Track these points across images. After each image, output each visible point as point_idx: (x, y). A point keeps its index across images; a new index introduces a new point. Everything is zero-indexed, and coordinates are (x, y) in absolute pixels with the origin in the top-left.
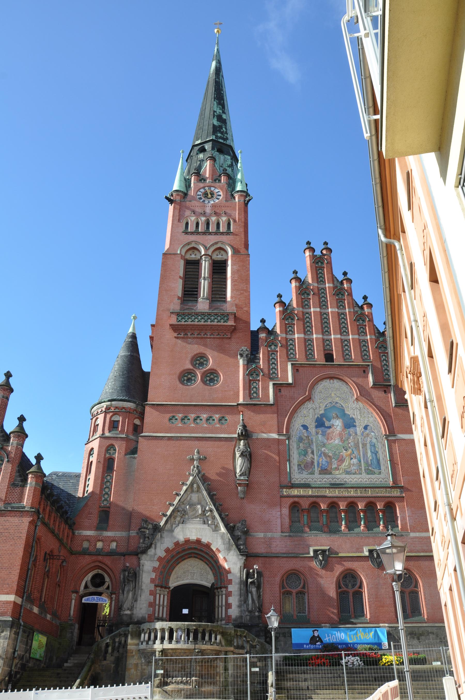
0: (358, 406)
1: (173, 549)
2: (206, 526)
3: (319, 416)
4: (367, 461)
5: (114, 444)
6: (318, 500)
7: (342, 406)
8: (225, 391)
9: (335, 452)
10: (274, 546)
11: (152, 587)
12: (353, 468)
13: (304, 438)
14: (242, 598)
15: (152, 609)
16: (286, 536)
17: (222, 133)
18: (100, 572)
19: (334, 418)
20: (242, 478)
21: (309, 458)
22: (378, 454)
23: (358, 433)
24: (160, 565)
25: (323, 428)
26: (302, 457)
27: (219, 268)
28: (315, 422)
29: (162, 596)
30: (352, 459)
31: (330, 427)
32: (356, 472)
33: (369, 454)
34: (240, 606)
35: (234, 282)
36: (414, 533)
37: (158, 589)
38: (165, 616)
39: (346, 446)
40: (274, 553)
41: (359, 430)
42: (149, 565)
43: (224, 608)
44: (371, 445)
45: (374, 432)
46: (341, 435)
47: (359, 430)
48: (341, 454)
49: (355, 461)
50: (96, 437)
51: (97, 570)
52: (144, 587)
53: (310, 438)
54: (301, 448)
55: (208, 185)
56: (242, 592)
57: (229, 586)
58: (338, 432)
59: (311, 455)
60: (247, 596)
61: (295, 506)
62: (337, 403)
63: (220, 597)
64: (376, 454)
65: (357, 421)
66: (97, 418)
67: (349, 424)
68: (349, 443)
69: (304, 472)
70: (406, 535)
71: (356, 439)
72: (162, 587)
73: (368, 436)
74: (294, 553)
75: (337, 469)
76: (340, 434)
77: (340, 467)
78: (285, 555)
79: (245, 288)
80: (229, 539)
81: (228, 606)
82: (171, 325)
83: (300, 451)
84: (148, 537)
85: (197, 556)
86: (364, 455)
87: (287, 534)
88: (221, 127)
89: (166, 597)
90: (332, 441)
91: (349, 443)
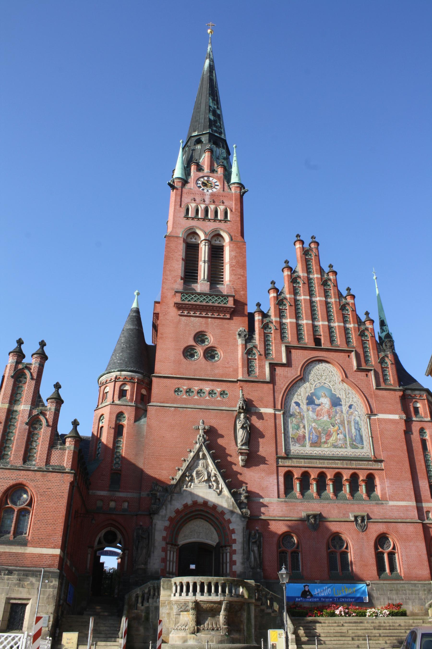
0: (343, 387)
1: (183, 511)
2: (211, 491)
3: (310, 395)
4: (352, 437)
5: (124, 411)
7: (330, 387)
8: (225, 367)
9: (324, 427)
10: (272, 510)
11: (163, 544)
12: (340, 443)
13: (297, 414)
14: (245, 556)
15: (164, 564)
16: (282, 501)
17: (216, 127)
18: (113, 529)
19: (322, 397)
20: (244, 447)
21: (301, 432)
22: (361, 431)
23: (344, 411)
24: (170, 525)
25: (313, 405)
26: (295, 431)
27: (216, 253)
28: (306, 400)
29: (172, 553)
30: (338, 434)
31: (319, 405)
32: (342, 446)
33: (353, 430)
34: (243, 563)
35: (232, 267)
36: (392, 502)
37: (169, 546)
38: (174, 571)
39: (334, 422)
40: (271, 516)
41: (345, 408)
42: (160, 525)
43: (228, 565)
44: (355, 423)
45: (357, 411)
46: (329, 413)
47: (345, 408)
48: (329, 429)
50: (106, 404)
51: (109, 528)
52: (157, 544)
53: (302, 414)
54: (294, 422)
55: (207, 175)
56: (245, 550)
57: (234, 545)
58: (326, 409)
59: (303, 430)
60: (249, 554)
62: (325, 383)
63: (225, 555)
64: (359, 431)
65: (342, 401)
66: (106, 386)
67: (336, 402)
68: (336, 420)
69: (297, 444)
70: (386, 503)
71: (342, 417)
72: (172, 545)
73: (352, 415)
74: (290, 517)
75: (326, 443)
76: (328, 412)
77: (328, 441)
78: (282, 519)
79: (242, 274)
80: (233, 503)
81: (233, 563)
82: (175, 303)
83: (293, 425)
84: (159, 499)
85: (203, 517)
86: (349, 431)
87: (283, 500)
88: (215, 121)
89: (175, 553)
90: (321, 417)
91: (336, 420)
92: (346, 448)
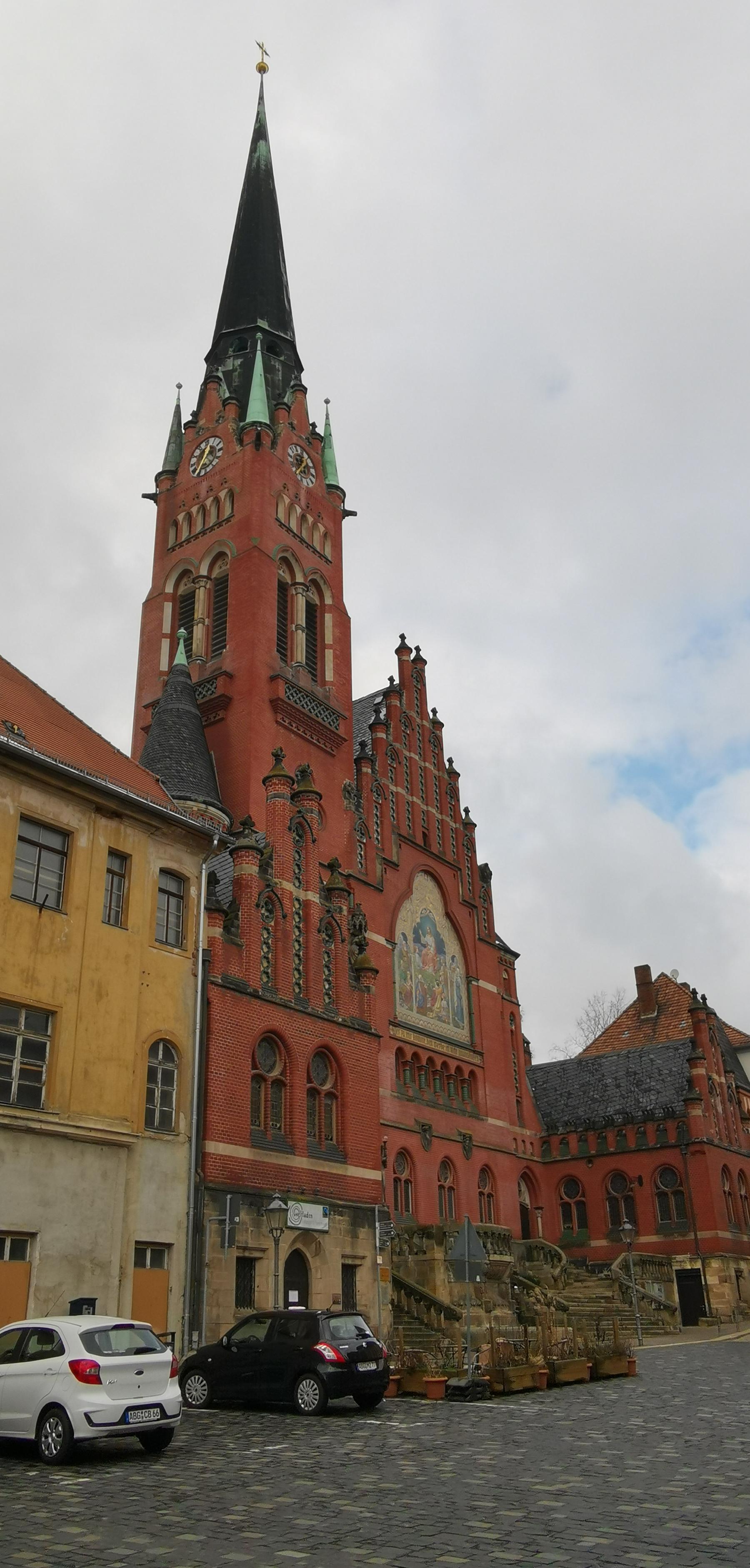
6: (420, 1051)
49: (444, 1003)
61: (400, 1052)
67: (440, 948)
92: (449, 1023)
